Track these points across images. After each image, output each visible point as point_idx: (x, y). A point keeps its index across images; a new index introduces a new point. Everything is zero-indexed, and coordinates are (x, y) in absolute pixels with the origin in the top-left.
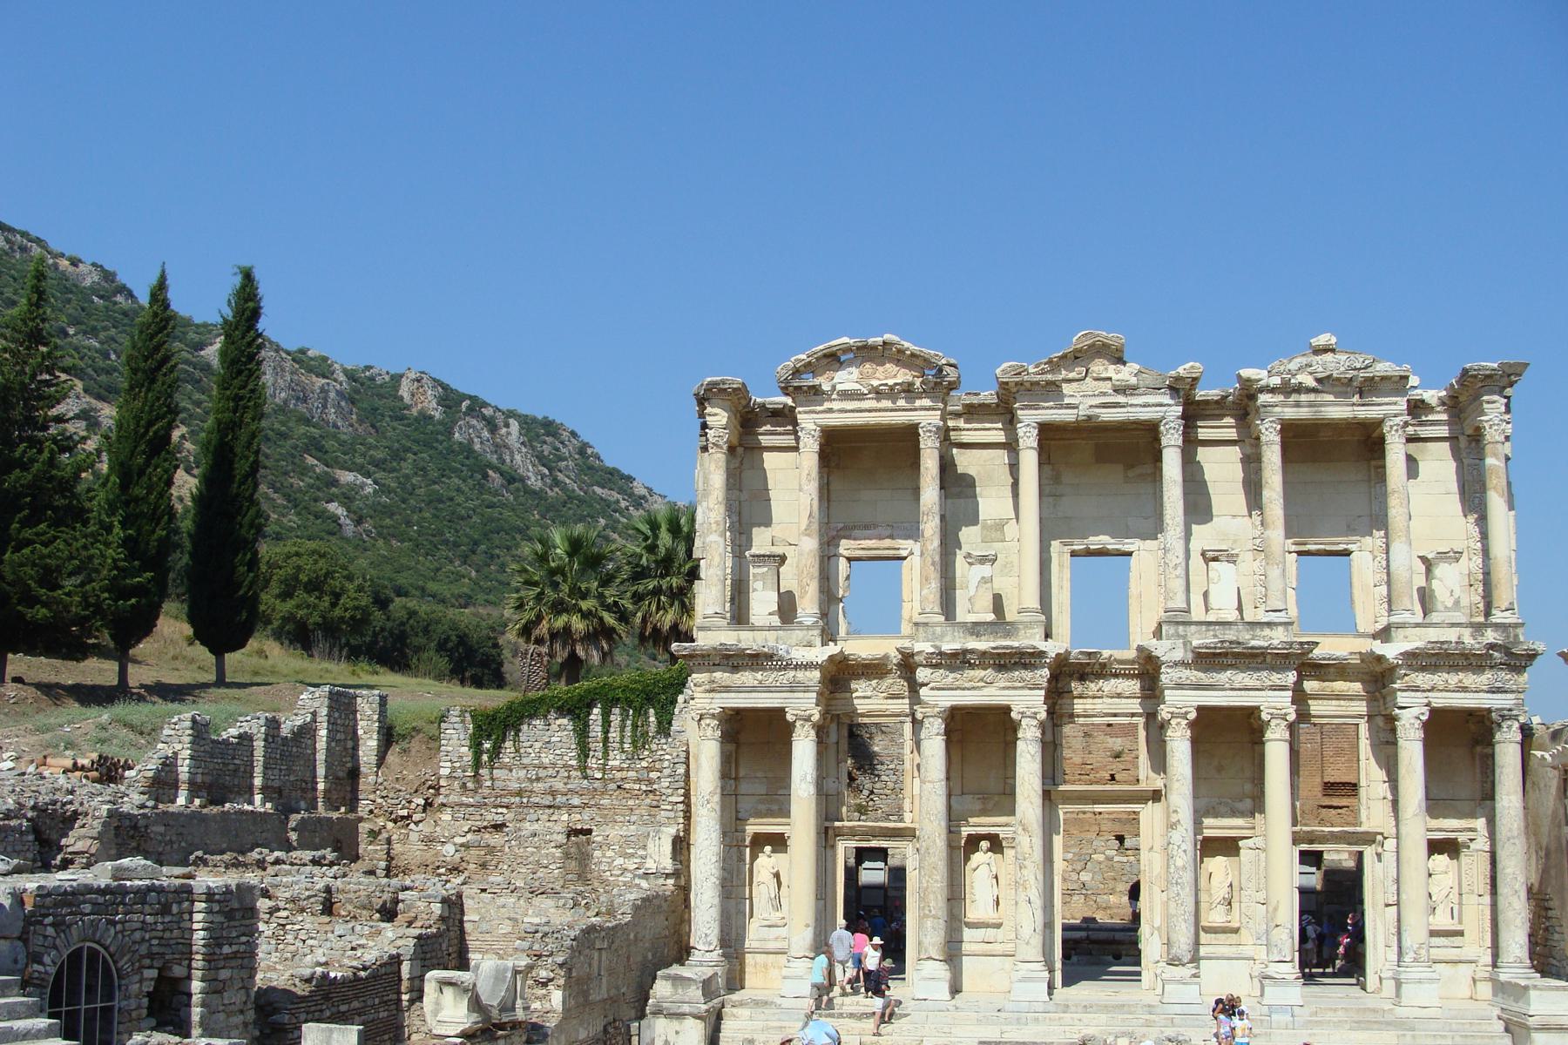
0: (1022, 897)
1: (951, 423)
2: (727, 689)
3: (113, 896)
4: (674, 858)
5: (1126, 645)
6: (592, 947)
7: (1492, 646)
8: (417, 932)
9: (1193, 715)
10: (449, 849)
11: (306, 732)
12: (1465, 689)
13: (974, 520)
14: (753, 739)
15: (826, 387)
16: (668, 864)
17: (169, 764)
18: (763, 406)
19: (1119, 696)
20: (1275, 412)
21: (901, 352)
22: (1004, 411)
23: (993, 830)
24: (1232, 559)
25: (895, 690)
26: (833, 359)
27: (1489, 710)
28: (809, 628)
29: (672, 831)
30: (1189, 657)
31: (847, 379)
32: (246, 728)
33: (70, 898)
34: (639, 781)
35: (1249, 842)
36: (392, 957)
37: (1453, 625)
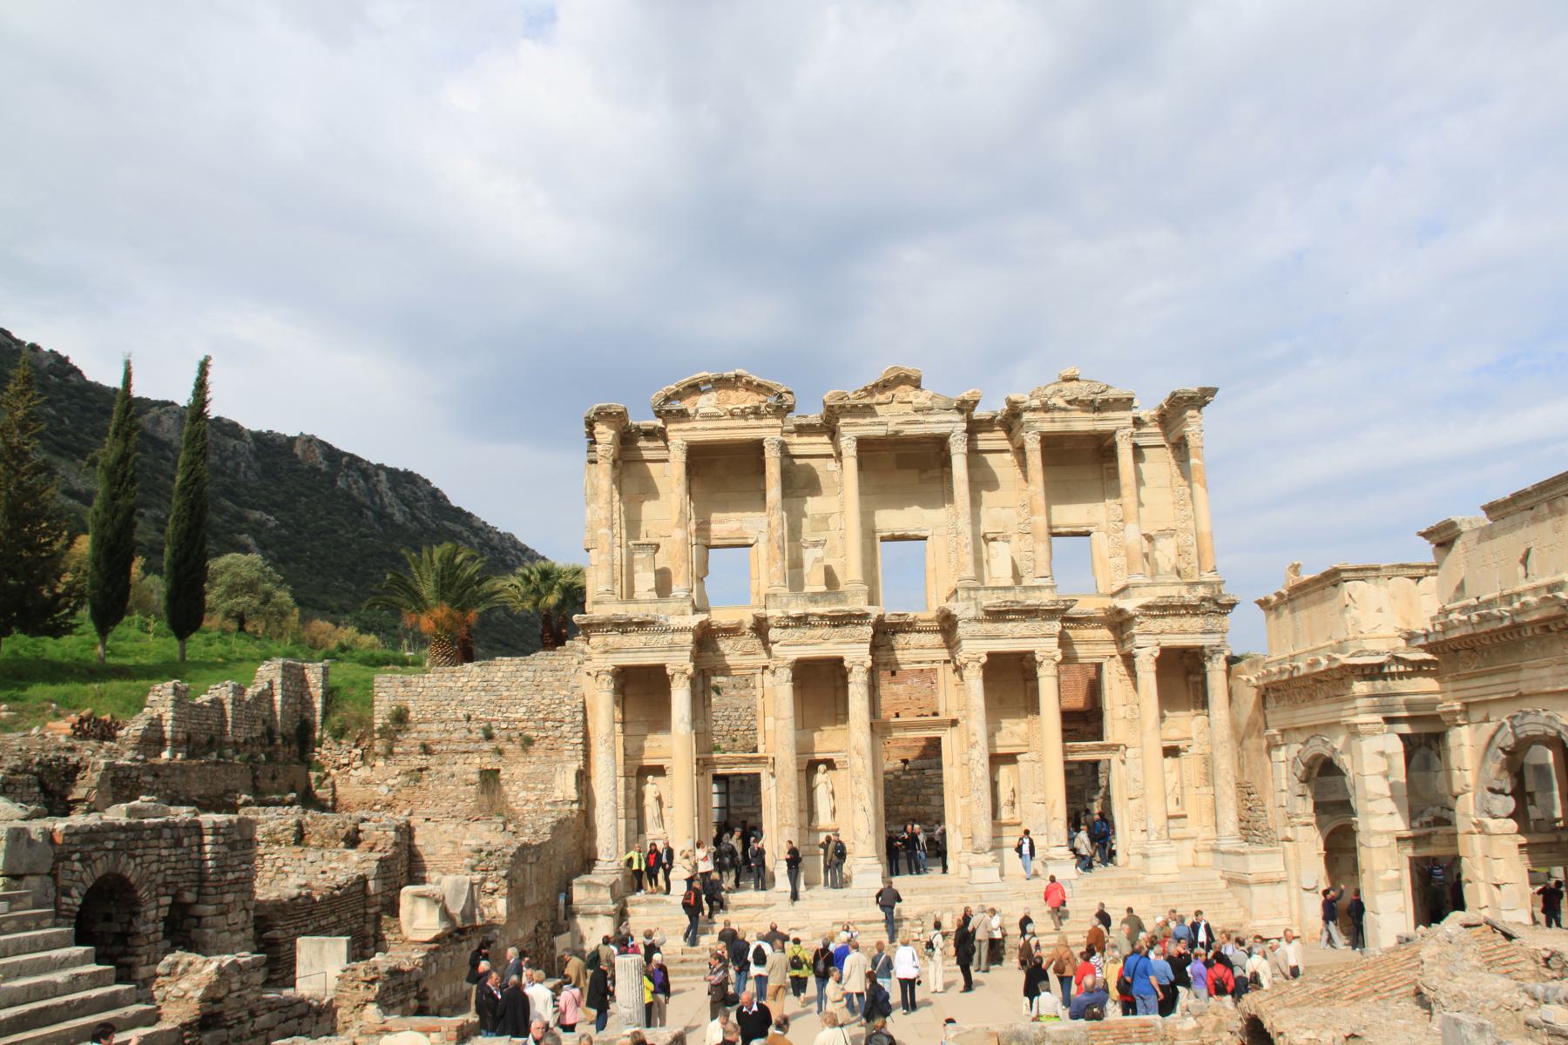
0: (858, 806)
1: (786, 440)
2: (618, 650)
3: (133, 833)
4: (577, 788)
5: (927, 608)
6: (525, 862)
7: (1203, 599)
8: (379, 855)
9: (984, 660)
10: (383, 789)
11: (266, 696)
12: (1185, 632)
13: (805, 515)
14: (641, 690)
15: (691, 411)
16: (573, 795)
17: (156, 724)
18: (638, 428)
19: (922, 647)
20: (1036, 427)
21: (749, 383)
22: (829, 427)
23: (828, 756)
24: (1007, 540)
25: (749, 648)
26: (694, 388)
27: (1202, 648)
28: (682, 600)
29: (575, 766)
30: (981, 615)
31: (706, 403)
32: (216, 694)
33: (91, 836)
34: (537, 729)
35: (1025, 756)
36: (359, 877)
37: (1175, 584)
